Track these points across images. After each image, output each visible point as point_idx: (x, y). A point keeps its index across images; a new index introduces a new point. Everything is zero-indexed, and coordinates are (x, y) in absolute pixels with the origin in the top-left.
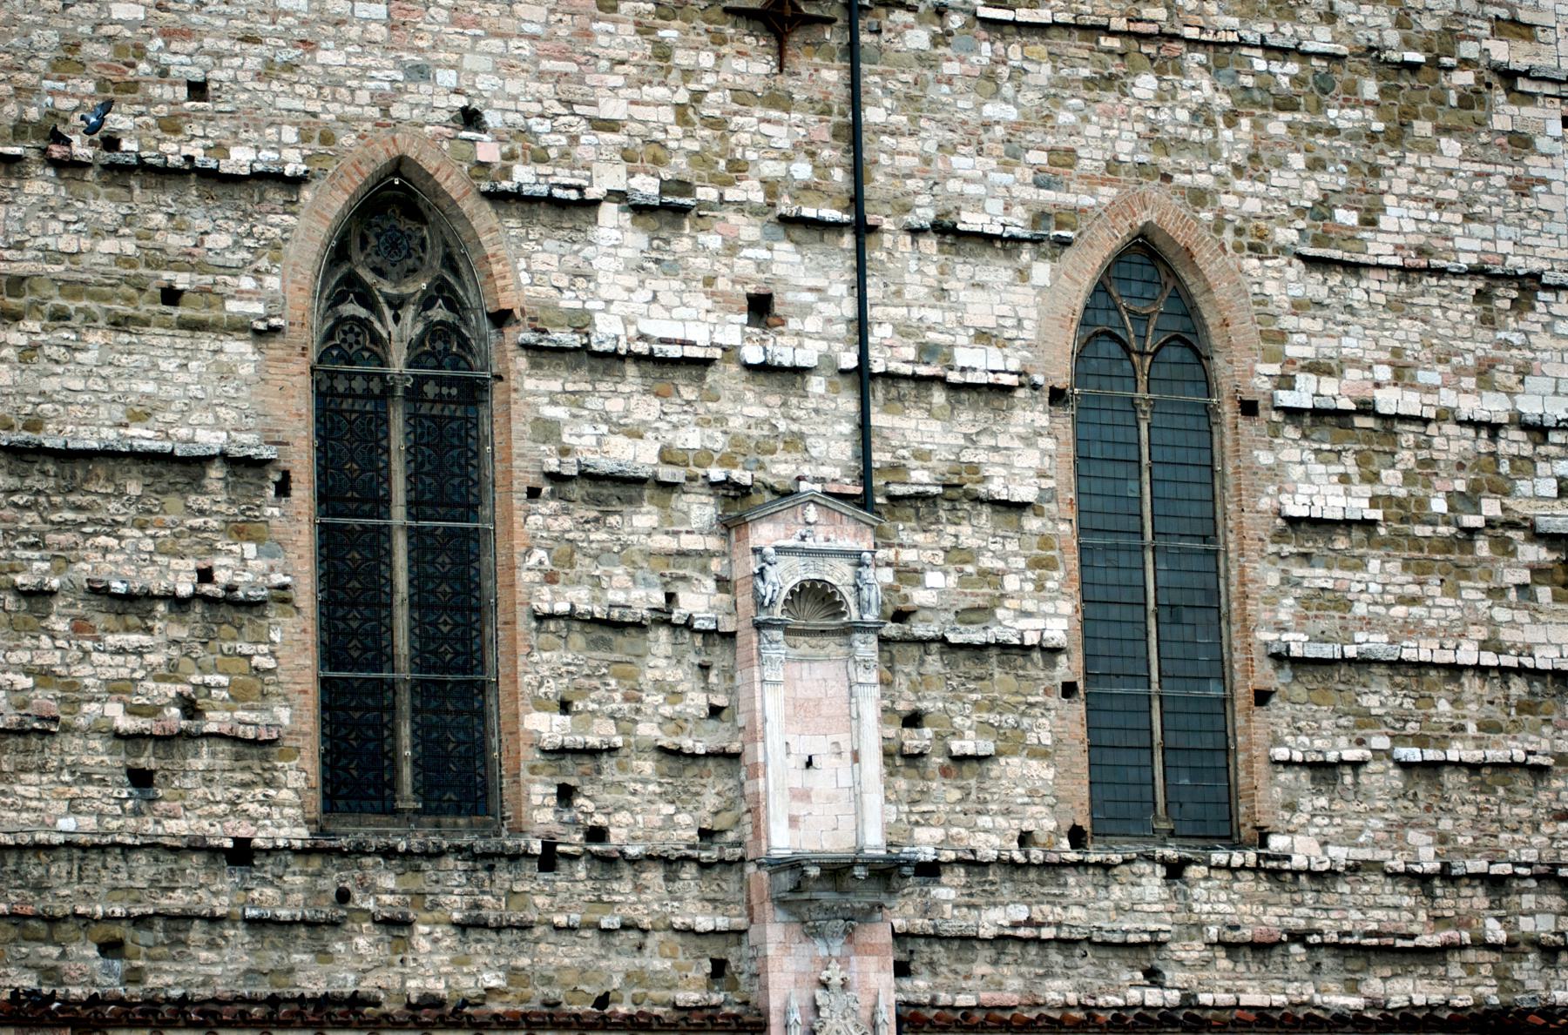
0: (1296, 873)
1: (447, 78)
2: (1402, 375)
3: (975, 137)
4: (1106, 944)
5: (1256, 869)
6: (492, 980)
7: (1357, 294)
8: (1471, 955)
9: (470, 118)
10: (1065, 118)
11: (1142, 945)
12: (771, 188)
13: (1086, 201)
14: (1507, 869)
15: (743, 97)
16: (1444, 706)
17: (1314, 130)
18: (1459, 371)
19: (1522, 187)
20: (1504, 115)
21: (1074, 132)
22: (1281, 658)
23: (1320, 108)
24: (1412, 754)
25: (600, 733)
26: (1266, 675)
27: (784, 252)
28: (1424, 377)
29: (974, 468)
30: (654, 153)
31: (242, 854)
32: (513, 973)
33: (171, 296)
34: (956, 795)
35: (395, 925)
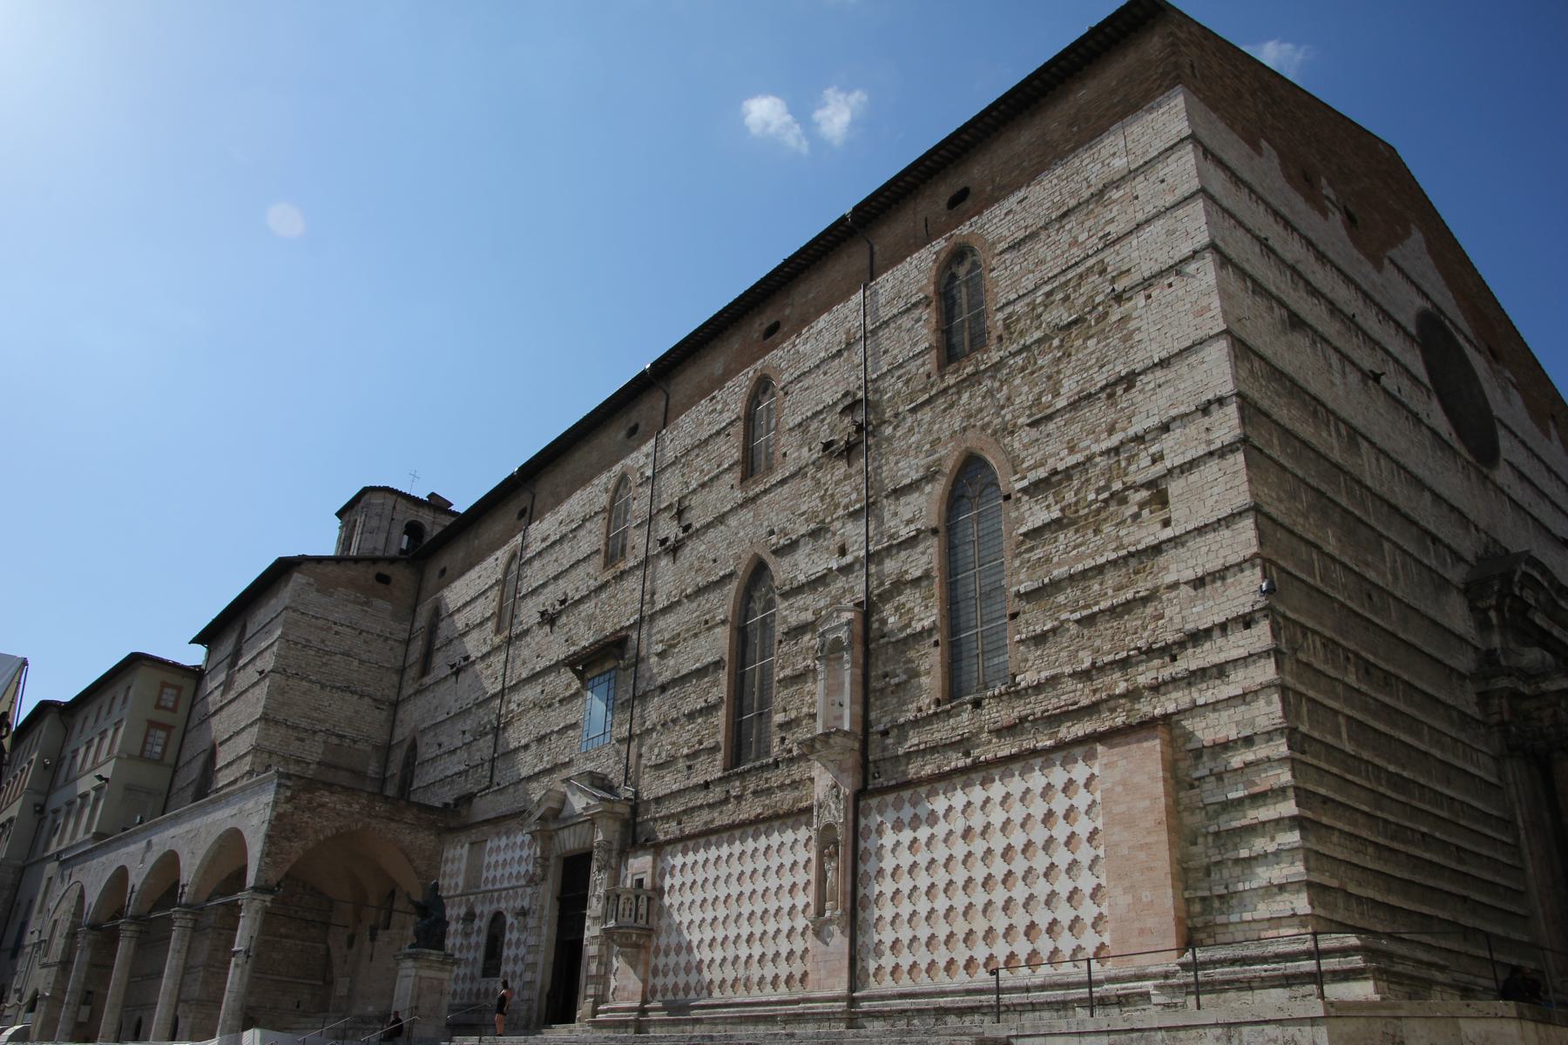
0: (1026, 689)
1: (765, 524)
2: (1072, 450)
3: (906, 454)
4: (945, 745)
5: (1008, 693)
6: (759, 810)
7: (1051, 426)
8: (1112, 704)
9: (772, 533)
10: (937, 426)
11: (960, 742)
12: (846, 507)
13: (943, 453)
14: (1124, 654)
15: (837, 483)
16: (1096, 587)
17: (1032, 373)
18: (1101, 432)
19: (1130, 335)
20: (1116, 314)
21: (940, 428)
22: (1018, 595)
23: (1035, 363)
24: (1077, 615)
25: (793, 715)
26: (1015, 606)
27: (849, 526)
28: (1082, 445)
29: (906, 572)
30: (815, 514)
31: (706, 785)
32: (764, 806)
33: (706, 622)
34: (895, 700)
35: (739, 798)
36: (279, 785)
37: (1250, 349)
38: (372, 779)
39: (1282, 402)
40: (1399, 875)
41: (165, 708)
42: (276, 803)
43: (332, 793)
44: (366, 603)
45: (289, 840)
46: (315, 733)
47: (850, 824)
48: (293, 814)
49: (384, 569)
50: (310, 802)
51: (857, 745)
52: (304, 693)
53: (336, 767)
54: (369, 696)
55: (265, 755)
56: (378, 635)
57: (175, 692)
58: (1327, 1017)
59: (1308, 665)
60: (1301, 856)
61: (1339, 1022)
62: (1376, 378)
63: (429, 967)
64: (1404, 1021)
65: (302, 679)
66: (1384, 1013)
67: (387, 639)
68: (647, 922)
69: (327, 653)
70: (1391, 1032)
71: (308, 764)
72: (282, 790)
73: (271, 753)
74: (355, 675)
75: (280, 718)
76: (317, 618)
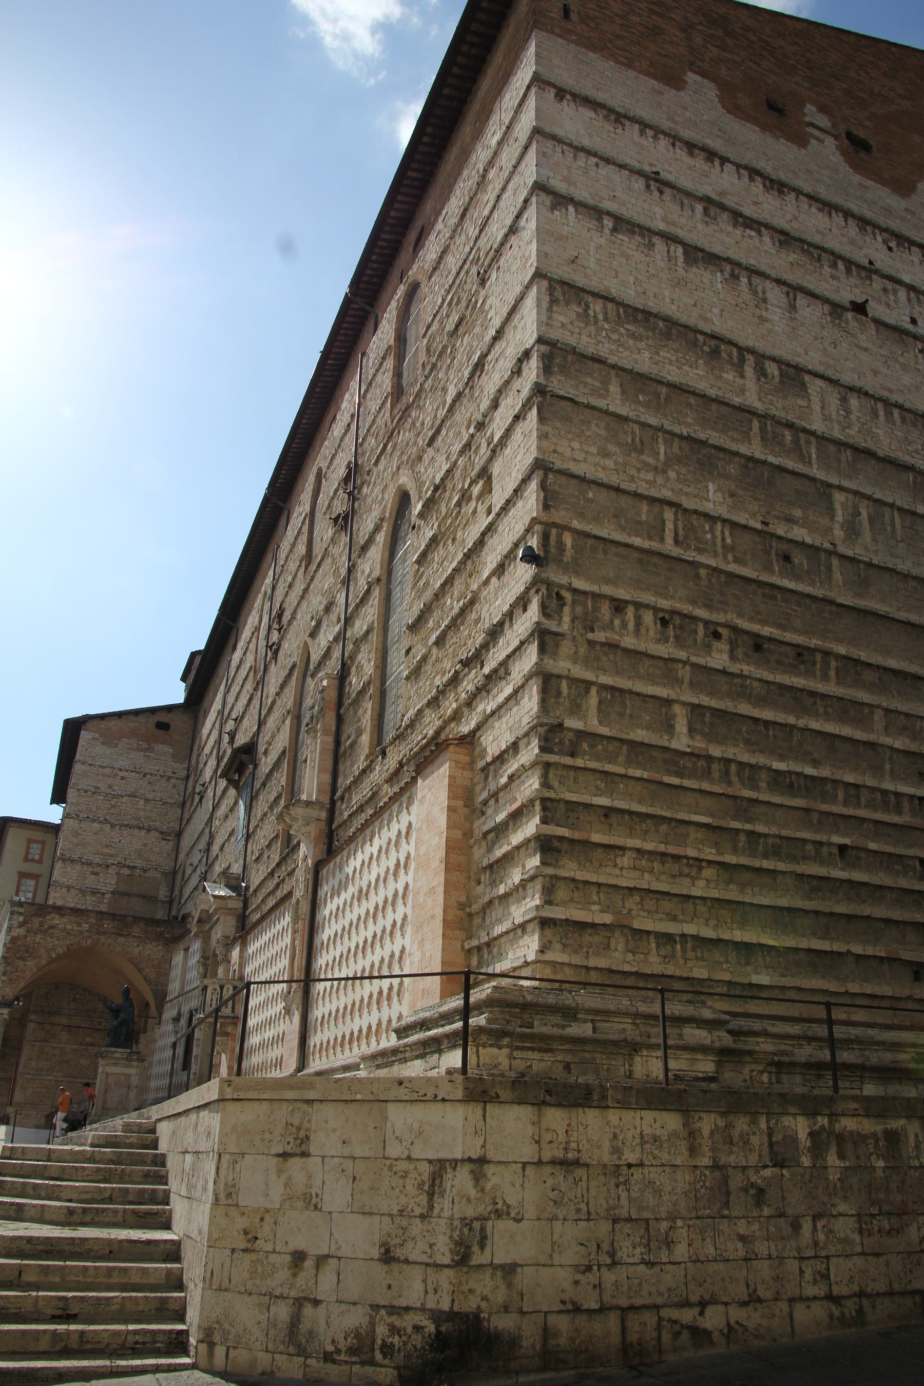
36: (12, 913)
37: (583, 290)
38: (162, 902)
39: (642, 345)
40: (766, 901)
41: (33, 860)
42: (10, 929)
43: (62, 915)
44: (147, 749)
45: (23, 959)
46: (107, 867)
47: (310, 896)
48: (26, 937)
49: (164, 718)
50: (41, 925)
51: (324, 815)
52: (96, 833)
53: (128, 895)
54: (156, 830)
55: (64, 890)
56: (162, 776)
57: (40, 846)
58: (221, 1100)
59: (613, 646)
60: (539, 887)
61: (231, 1106)
62: (860, 308)
63: (116, 1064)
64: (316, 1106)
65: (93, 821)
66: (290, 1095)
67: (169, 778)
68: (233, 1011)
69: (114, 796)
70: (296, 1123)
71: (103, 894)
72: (15, 917)
73: (69, 888)
74: (141, 813)
75: (76, 857)
76: (103, 767)
